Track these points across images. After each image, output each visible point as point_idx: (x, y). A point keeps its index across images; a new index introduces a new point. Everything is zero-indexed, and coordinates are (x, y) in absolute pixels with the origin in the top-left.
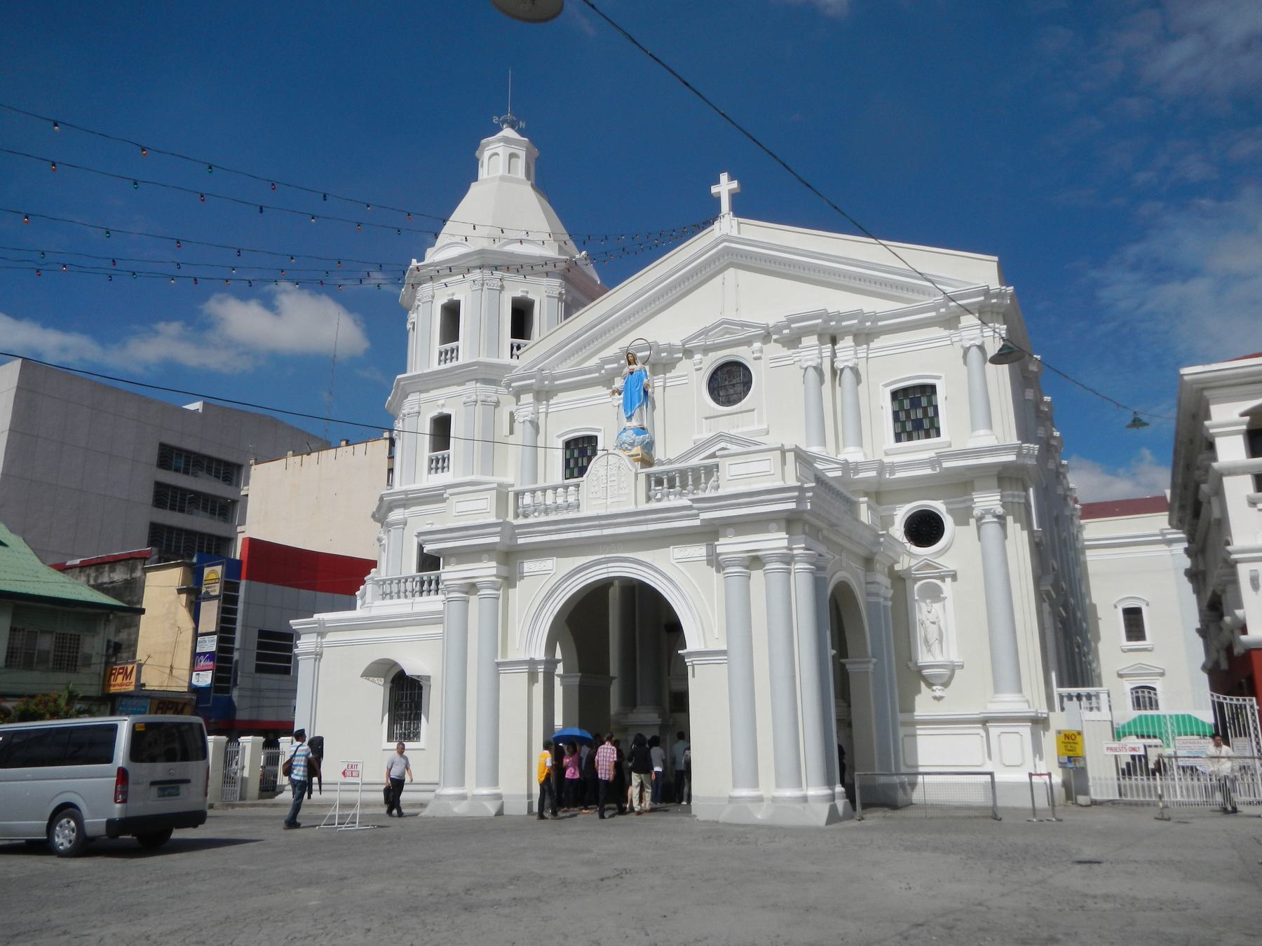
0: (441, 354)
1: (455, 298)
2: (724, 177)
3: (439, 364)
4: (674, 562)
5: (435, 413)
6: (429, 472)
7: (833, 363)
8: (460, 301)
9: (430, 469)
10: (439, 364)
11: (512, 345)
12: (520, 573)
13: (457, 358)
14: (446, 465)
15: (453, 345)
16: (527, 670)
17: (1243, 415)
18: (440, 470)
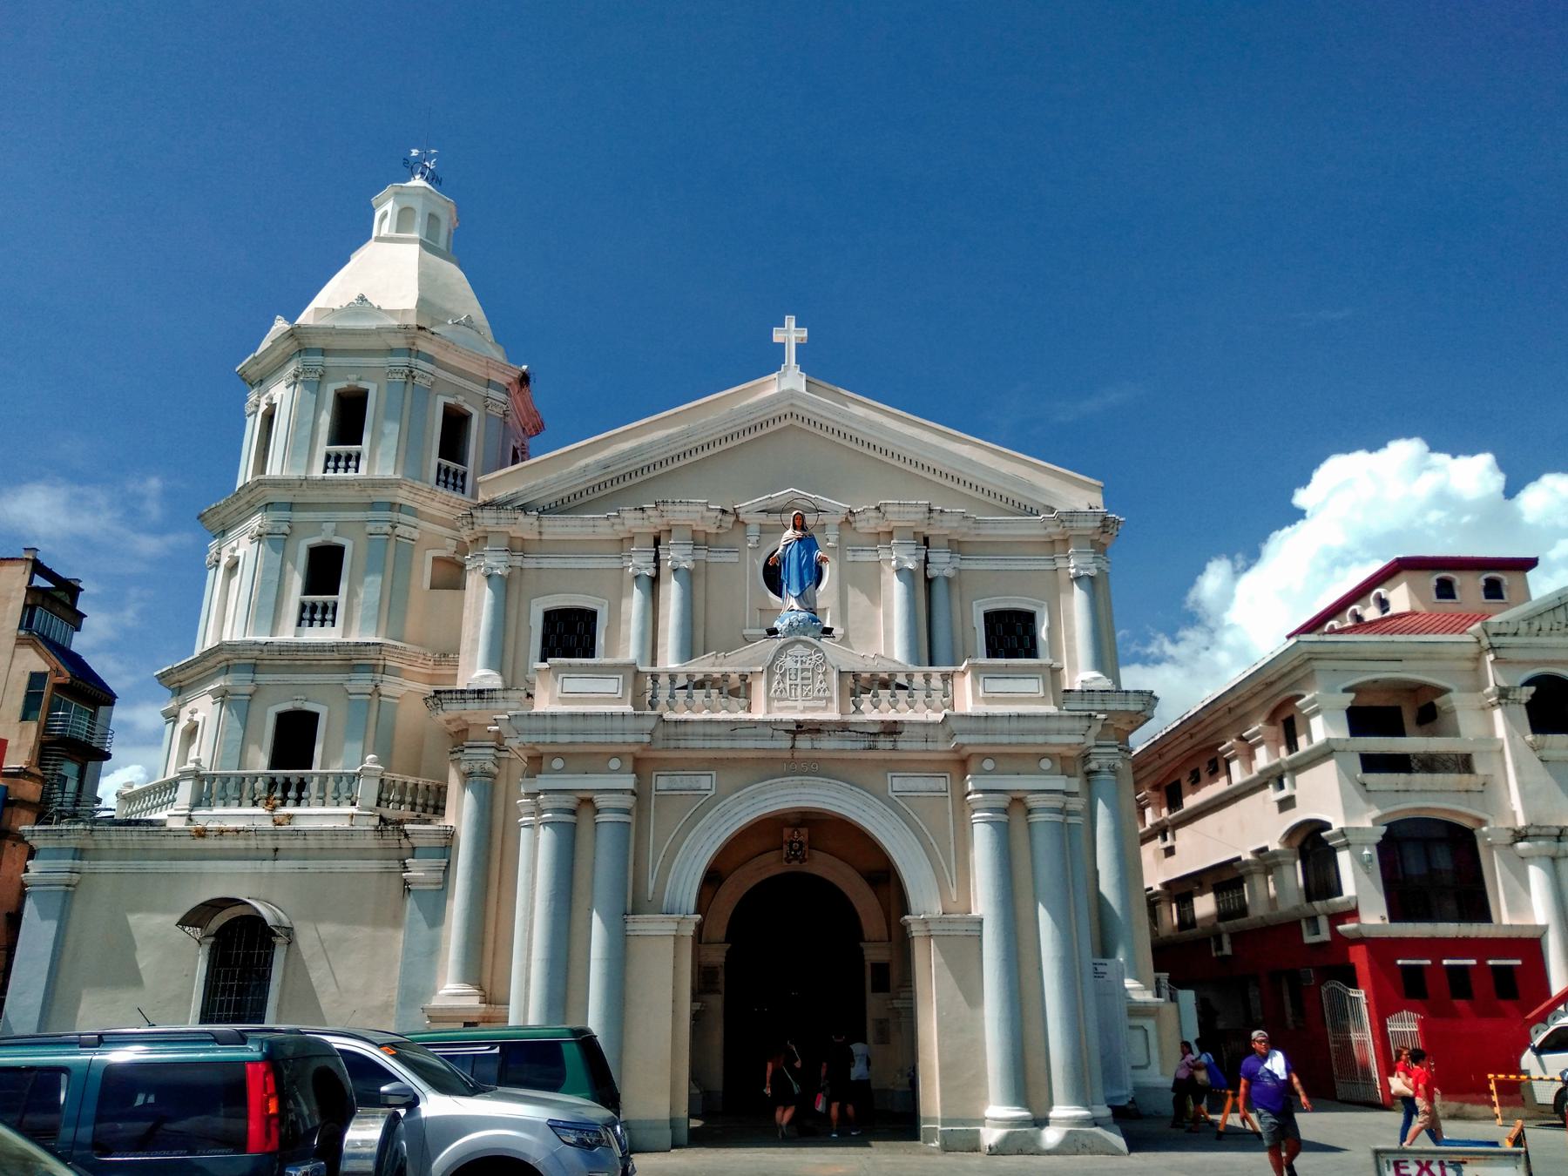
0: (328, 457)
1: (363, 385)
2: (791, 321)
3: (325, 472)
4: (893, 795)
5: (316, 541)
6: (299, 625)
7: (926, 569)
8: (368, 390)
9: (301, 619)
10: (325, 472)
11: (439, 465)
12: (656, 790)
13: (357, 471)
14: (329, 616)
15: (353, 448)
16: (674, 933)
17: (1346, 690)
18: (317, 623)
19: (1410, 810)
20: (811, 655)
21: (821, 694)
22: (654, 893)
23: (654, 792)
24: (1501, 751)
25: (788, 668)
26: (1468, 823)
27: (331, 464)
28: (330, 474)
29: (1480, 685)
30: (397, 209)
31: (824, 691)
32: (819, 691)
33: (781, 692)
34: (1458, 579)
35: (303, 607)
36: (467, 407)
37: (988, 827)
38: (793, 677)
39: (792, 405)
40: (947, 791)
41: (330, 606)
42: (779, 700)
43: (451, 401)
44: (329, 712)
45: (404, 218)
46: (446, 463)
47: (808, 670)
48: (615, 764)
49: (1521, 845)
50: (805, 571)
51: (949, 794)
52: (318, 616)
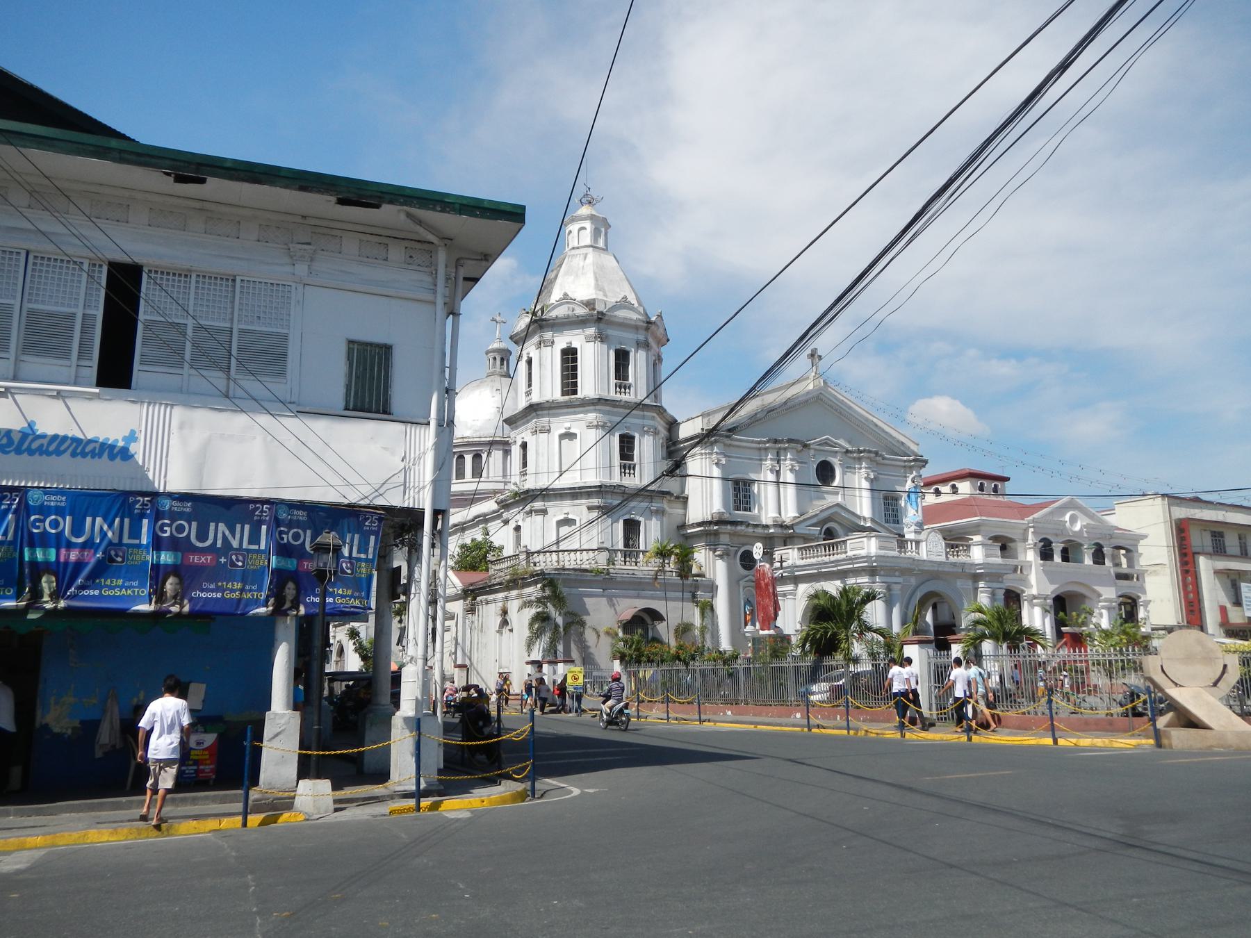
14: (632, 472)
18: (627, 475)
19: (1013, 587)
24: (1031, 566)
26: (1019, 592)
27: (618, 389)
28: (618, 395)
29: (1025, 540)
30: (593, 227)
34: (986, 483)
37: (988, 599)
39: (821, 393)
41: (632, 466)
45: (596, 233)
48: (897, 573)
49: (1035, 601)
52: (627, 471)
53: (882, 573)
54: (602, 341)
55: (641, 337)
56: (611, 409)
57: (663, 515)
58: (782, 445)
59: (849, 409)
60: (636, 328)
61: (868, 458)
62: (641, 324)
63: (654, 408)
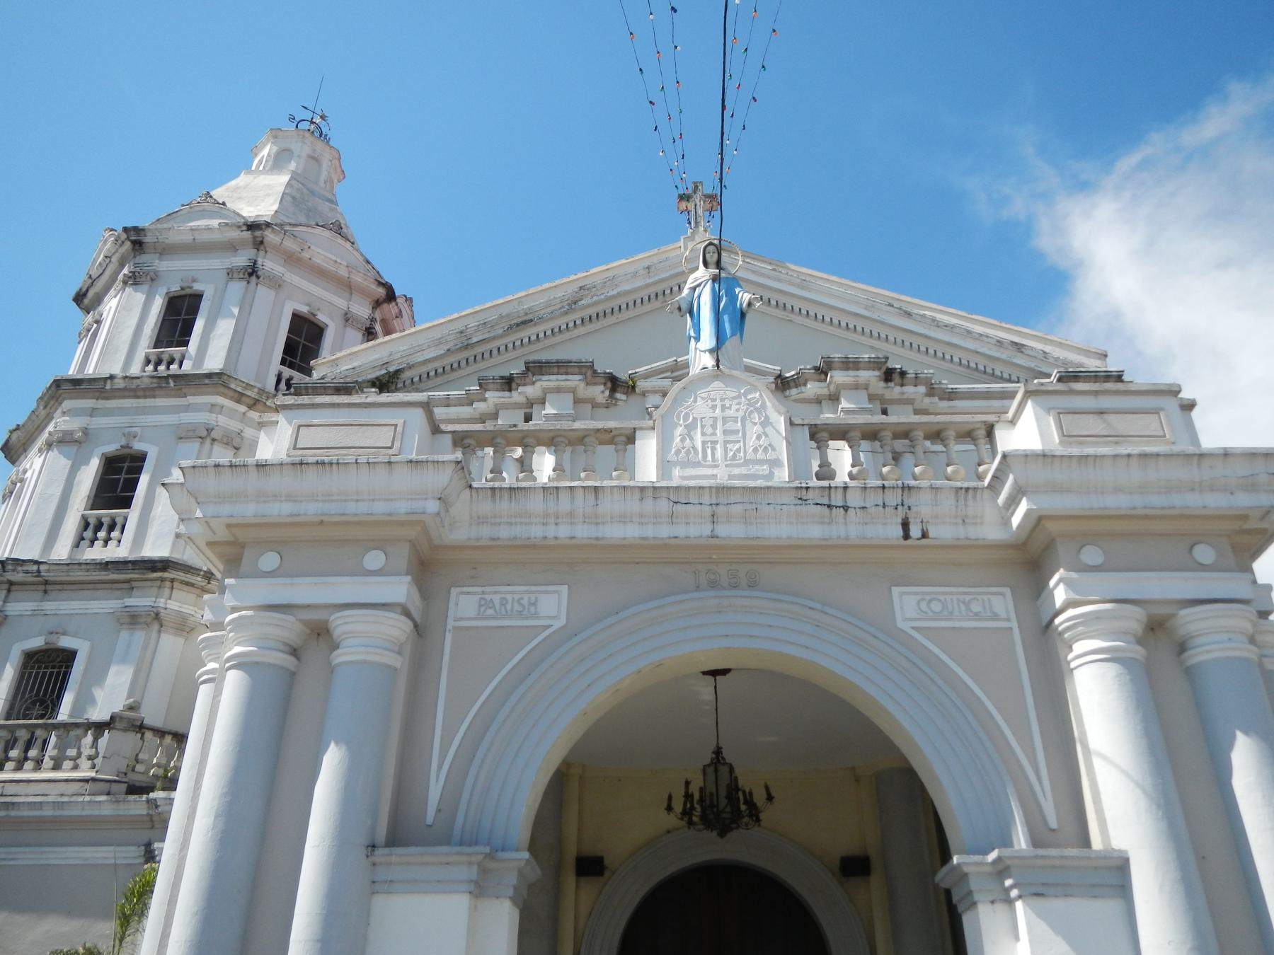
1: (197, 287)
14: (115, 534)
15: (175, 351)
20: (739, 397)
21: (760, 455)
22: (439, 811)
23: (451, 624)
25: (699, 417)
30: (275, 149)
31: (765, 450)
32: (755, 450)
33: (688, 452)
35: (86, 524)
36: (322, 317)
37: (1112, 669)
38: (709, 430)
40: (1008, 620)
42: (684, 465)
43: (304, 309)
44: (92, 649)
46: (287, 372)
47: (735, 419)
48: (375, 559)
50: (726, 318)
51: (1014, 624)
53: (270, 560)
54: (136, 283)
55: (241, 260)
56: (101, 404)
57: (160, 632)
58: (531, 391)
59: (803, 288)
60: (232, 247)
61: (856, 387)
62: (235, 234)
63: (207, 381)
